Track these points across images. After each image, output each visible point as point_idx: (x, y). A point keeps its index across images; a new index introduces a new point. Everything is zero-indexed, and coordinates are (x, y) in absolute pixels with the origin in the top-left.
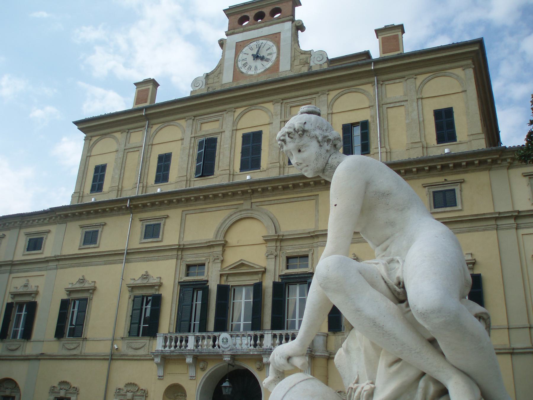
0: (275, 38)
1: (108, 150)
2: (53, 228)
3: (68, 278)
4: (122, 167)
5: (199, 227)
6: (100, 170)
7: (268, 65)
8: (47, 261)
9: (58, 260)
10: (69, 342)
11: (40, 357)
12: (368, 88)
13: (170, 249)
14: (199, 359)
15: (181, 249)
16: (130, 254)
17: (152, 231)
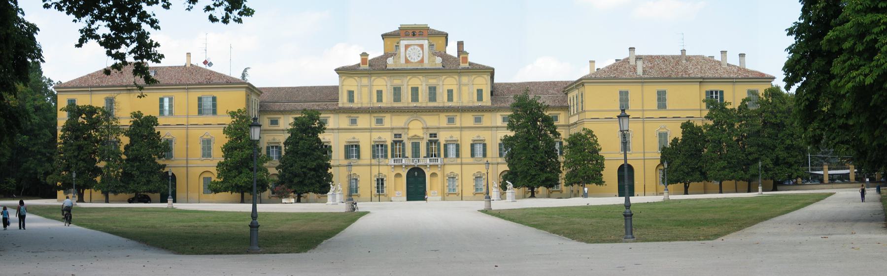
0: (422, 46)
1: (352, 84)
2: (331, 115)
3: (348, 137)
4: (361, 93)
5: (398, 121)
6: (351, 94)
7: (419, 59)
8: (332, 129)
9: (338, 129)
10: (354, 160)
11: (338, 166)
12: (456, 77)
13: (388, 129)
14: (406, 166)
15: (393, 129)
16: (371, 130)
17: (379, 121)
